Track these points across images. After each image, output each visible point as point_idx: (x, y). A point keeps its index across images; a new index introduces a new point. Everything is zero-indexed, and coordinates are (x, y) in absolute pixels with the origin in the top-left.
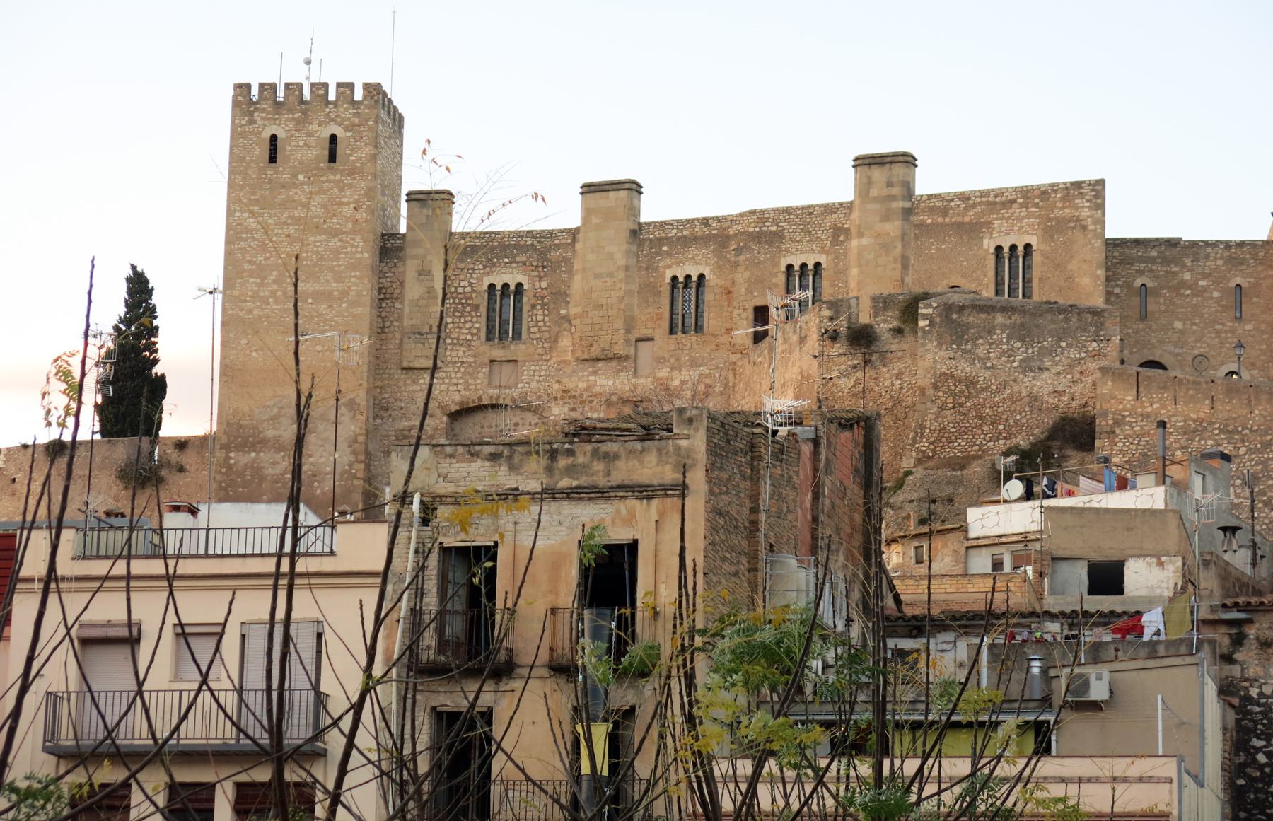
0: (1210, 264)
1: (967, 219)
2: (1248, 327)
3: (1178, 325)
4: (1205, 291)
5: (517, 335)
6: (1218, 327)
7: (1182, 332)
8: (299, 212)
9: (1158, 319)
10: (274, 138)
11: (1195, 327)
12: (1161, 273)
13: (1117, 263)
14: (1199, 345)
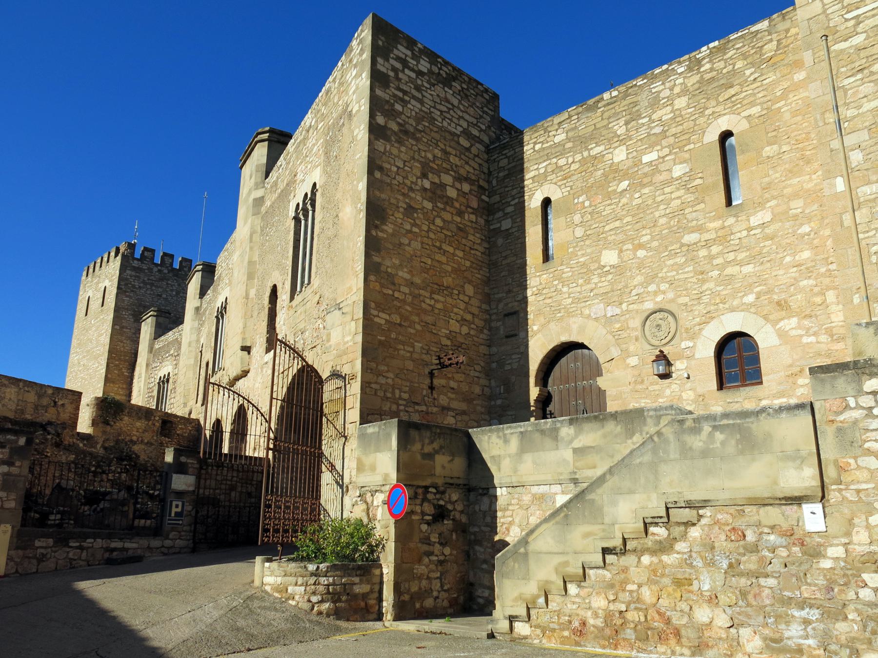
0: (665, 114)
3: (610, 257)
4: (657, 171)
7: (619, 269)
11: (641, 253)
12: (574, 167)
13: (505, 177)
14: (652, 288)
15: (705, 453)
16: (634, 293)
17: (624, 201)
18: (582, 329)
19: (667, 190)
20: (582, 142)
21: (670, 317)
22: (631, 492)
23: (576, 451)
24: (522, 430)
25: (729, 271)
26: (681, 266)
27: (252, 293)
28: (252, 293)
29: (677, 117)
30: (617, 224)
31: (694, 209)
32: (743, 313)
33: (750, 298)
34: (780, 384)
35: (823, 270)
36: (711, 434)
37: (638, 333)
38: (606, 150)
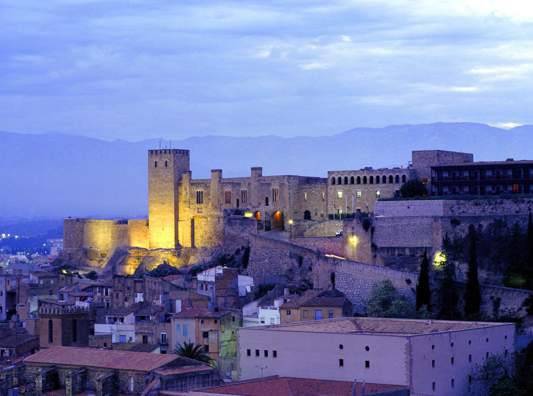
1: (268, 182)
5: (202, 203)
6: (320, 203)
7: (313, 204)
8: (161, 178)
10: (156, 162)
20: (310, 188)
27: (259, 195)
28: (259, 195)
29: (319, 190)
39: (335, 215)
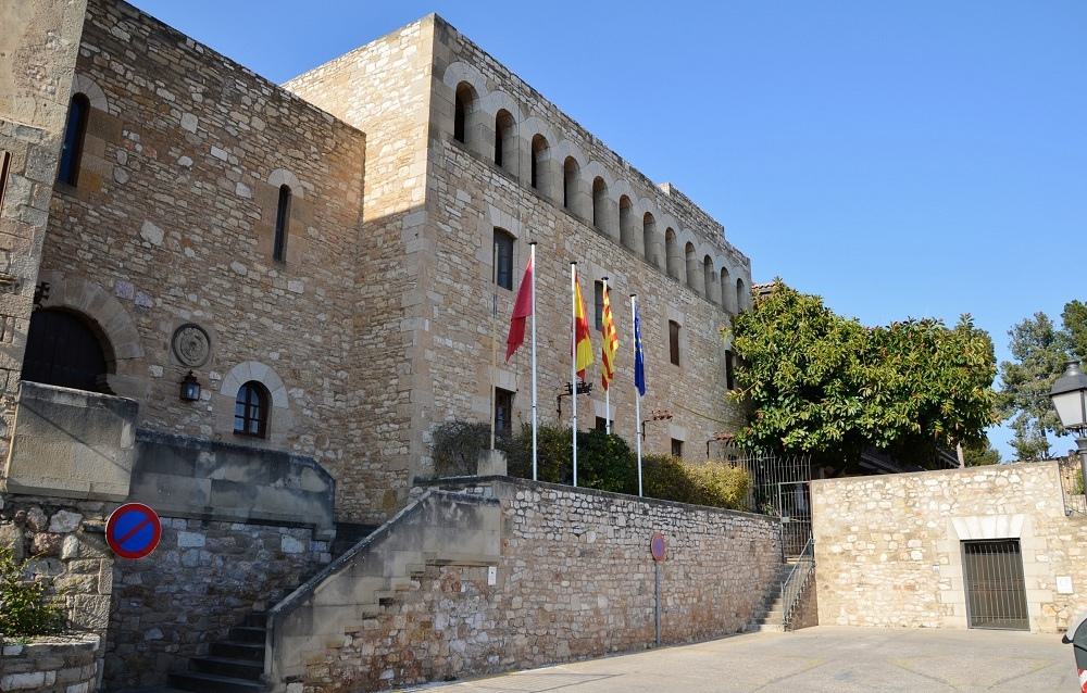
2: (295, 286)
6: (236, 266)
7: (160, 254)
9: (105, 199)
11: (189, 252)
14: (193, 297)
15: (452, 524)
16: (172, 291)
17: (182, 179)
18: (99, 302)
19: (230, 203)
21: (205, 339)
22: (405, 549)
23: (214, 482)
24: (148, 440)
25: (264, 320)
26: (225, 291)
30: (171, 200)
31: (248, 240)
32: (267, 367)
33: (275, 356)
34: (282, 444)
35: (326, 358)
36: (455, 510)
37: (168, 341)
38: (174, 102)
39: (540, 429)
